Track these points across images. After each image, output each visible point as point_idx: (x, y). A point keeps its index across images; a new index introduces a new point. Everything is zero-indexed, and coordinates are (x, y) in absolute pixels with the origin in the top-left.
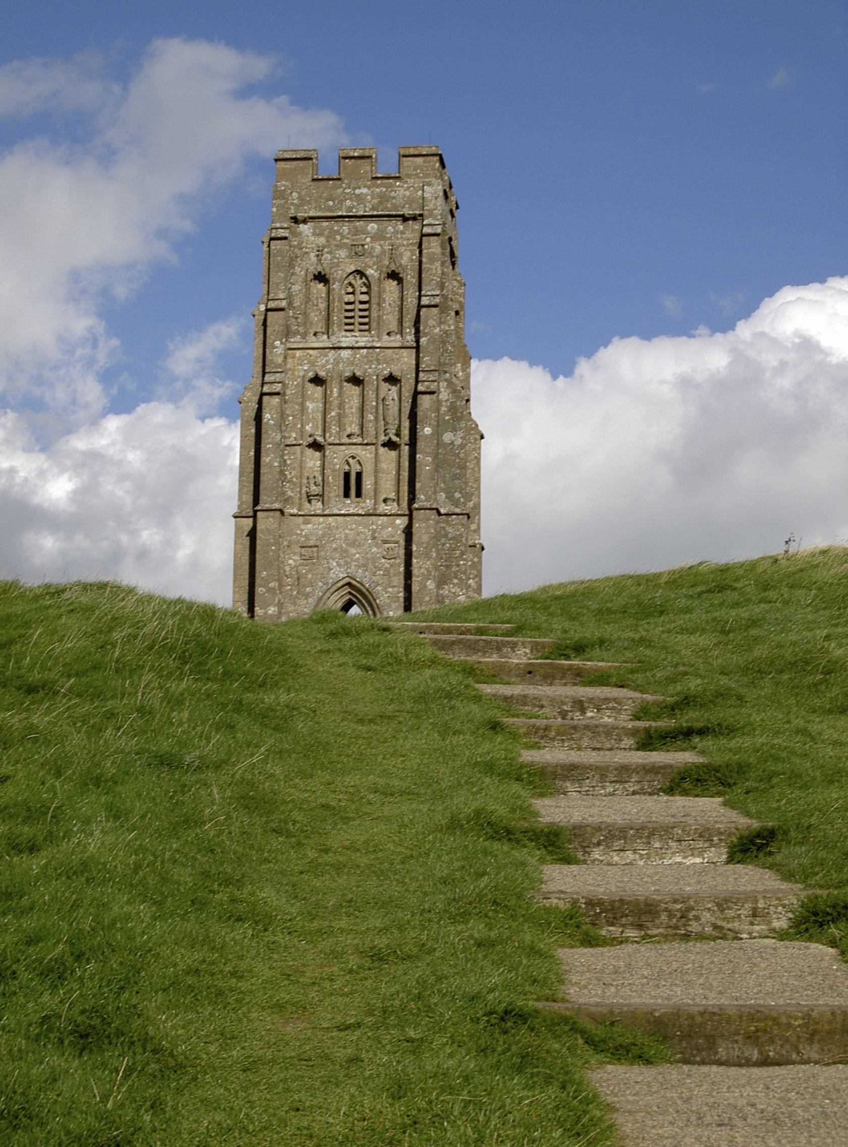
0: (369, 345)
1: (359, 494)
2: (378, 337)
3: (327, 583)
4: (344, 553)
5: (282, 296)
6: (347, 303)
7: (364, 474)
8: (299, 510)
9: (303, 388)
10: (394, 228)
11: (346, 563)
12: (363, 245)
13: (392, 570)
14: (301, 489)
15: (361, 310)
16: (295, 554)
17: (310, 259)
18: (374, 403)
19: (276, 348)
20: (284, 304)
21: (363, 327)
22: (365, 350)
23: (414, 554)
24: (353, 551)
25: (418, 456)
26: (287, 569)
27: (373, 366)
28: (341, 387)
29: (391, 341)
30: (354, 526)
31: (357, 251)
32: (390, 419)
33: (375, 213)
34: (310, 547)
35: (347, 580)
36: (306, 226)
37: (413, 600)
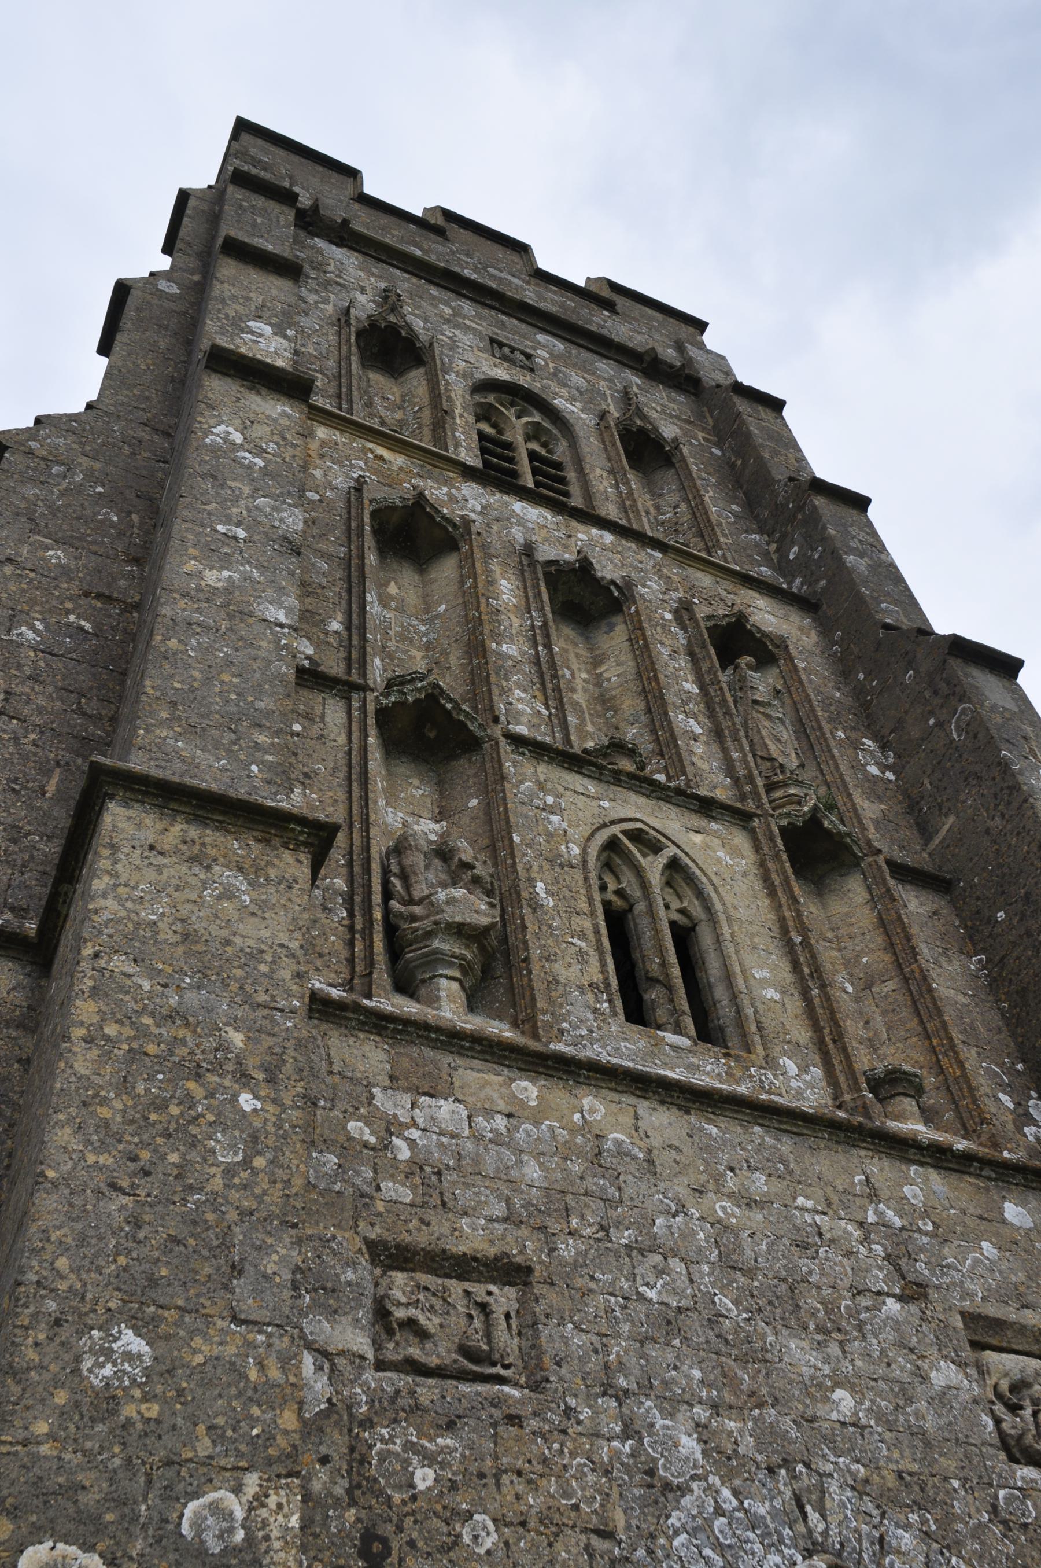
24: (800, 1355)
30: (760, 1183)
34: (464, 1267)
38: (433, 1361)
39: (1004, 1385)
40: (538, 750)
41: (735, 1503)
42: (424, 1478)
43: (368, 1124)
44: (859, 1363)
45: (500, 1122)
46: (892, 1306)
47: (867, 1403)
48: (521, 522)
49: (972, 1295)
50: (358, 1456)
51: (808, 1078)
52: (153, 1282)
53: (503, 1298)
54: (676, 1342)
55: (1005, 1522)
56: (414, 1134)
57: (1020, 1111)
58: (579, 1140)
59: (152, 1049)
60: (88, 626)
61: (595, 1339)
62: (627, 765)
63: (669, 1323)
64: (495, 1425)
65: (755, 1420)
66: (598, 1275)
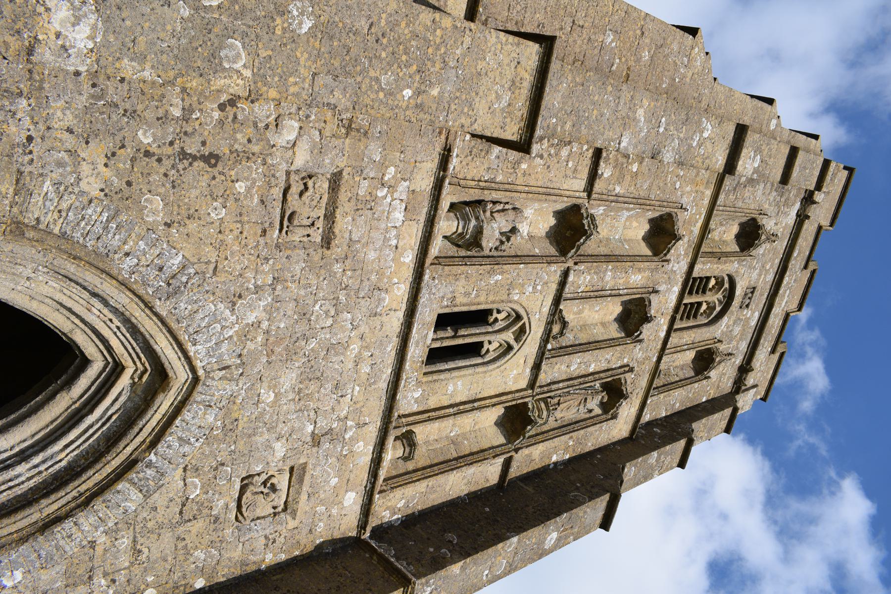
3: (173, 293)
4: (284, 348)
13: (198, 526)
16: (319, 150)
24: (289, 379)
30: (365, 369)
34: (330, 218)
35: (180, 374)
38: (289, 198)
39: (273, 480)
40: (563, 284)
41: (226, 336)
42: (240, 187)
43: (393, 177)
44: (285, 407)
45: (394, 242)
46: (310, 428)
47: (267, 409)
48: (669, 290)
49: (314, 469)
50: (249, 157)
51: (412, 402)
52: (331, 38)
54: (295, 317)
55: (216, 469)
56: (389, 199)
57: (396, 510)
58: (386, 280)
59: (430, 50)
60: (614, 68)
61: (298, 276)
62: (556, 329)
63: (304, 314)
64: (262, 223)
65: (261, 352)
66: (326, 282)
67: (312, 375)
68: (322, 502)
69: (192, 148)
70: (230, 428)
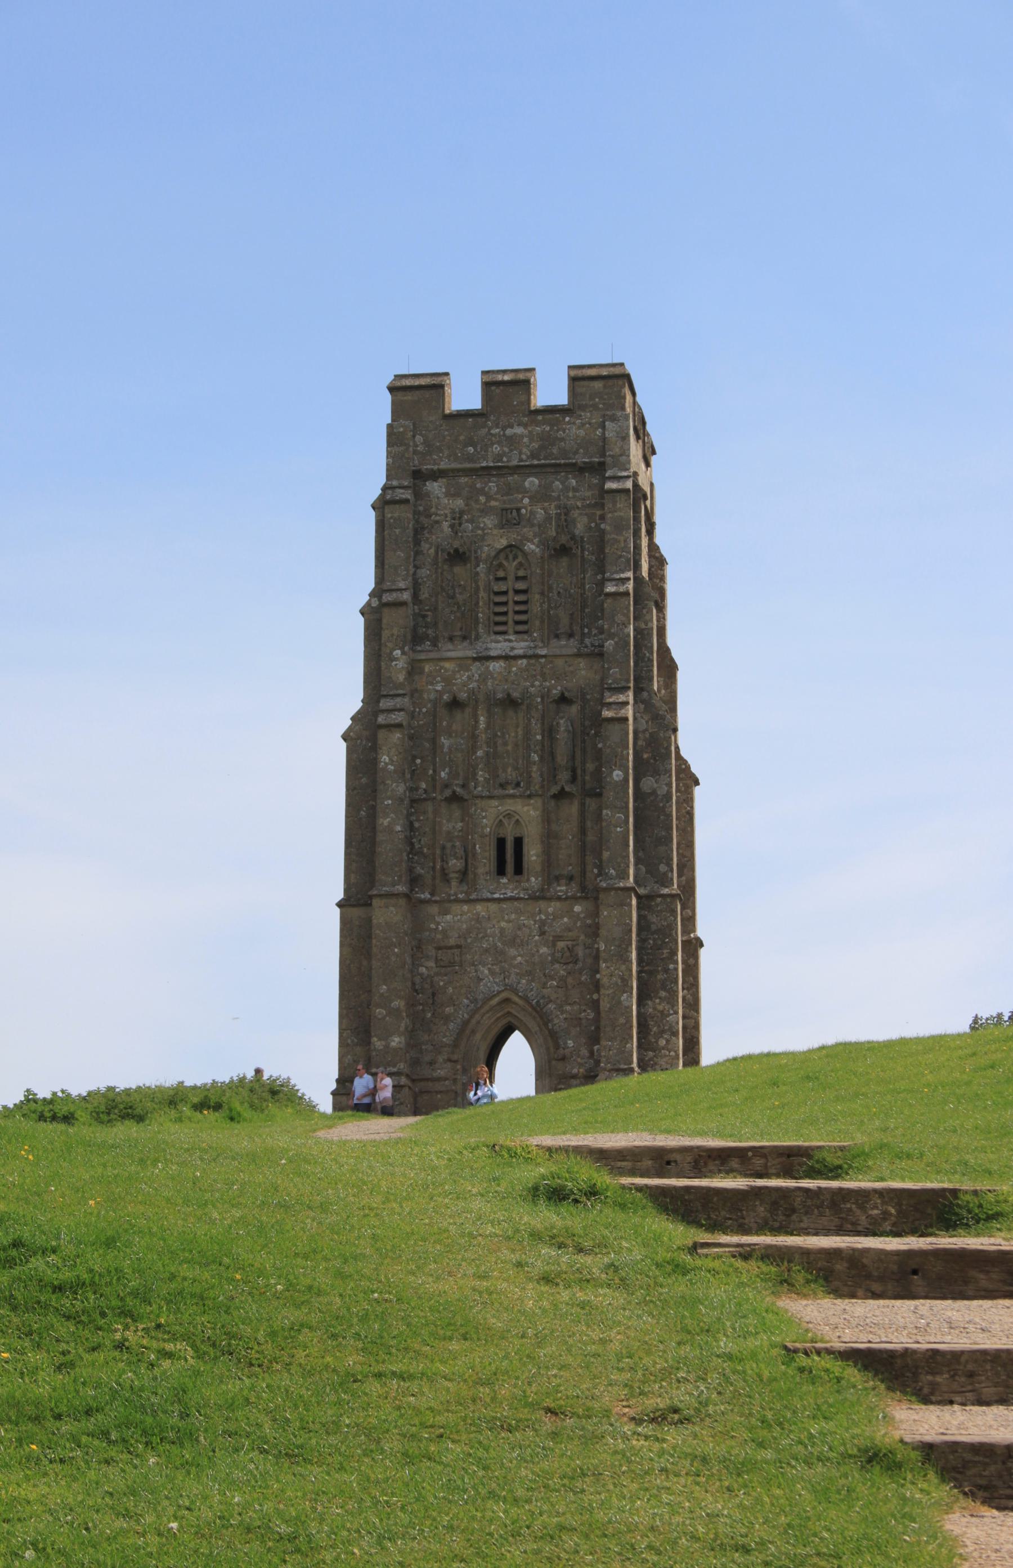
0: (530, 652)
1: (519, 870)
2: (542, 642)
5: (402, 585)
6: (497, 594)
7: (526, 841)
8: (432, 894)
9: (435, 717)
10: (562, 483)
11: (503, 971)
12: (518, 510)
13: (570, 980)
14: (434, 863)
15: (516, 603)
17: (442, 531)
18: (539, 737)
19: (396, 659)
20: (406, 596)
21: (520, 628)
22: (525, 661)
23: (602, 955)
24: (513, 952)
25: (604, 812)
26: (417, 980)
27: (537, 683)
28: (490, 715)
29: (561, 647)
31: (510, 518)
32: (562, 759)
33: (536, 462)
34: (451, 948)
36: (435, 484)
37: (602, 1023)
40: (482, 797)
42: (441, 984)
46: (537, 938)
50: (432, 982)
53: (456, 951)
67: (513, 942)
68: (575, 923)
69: (431, 1001)
70: (529, 973)
